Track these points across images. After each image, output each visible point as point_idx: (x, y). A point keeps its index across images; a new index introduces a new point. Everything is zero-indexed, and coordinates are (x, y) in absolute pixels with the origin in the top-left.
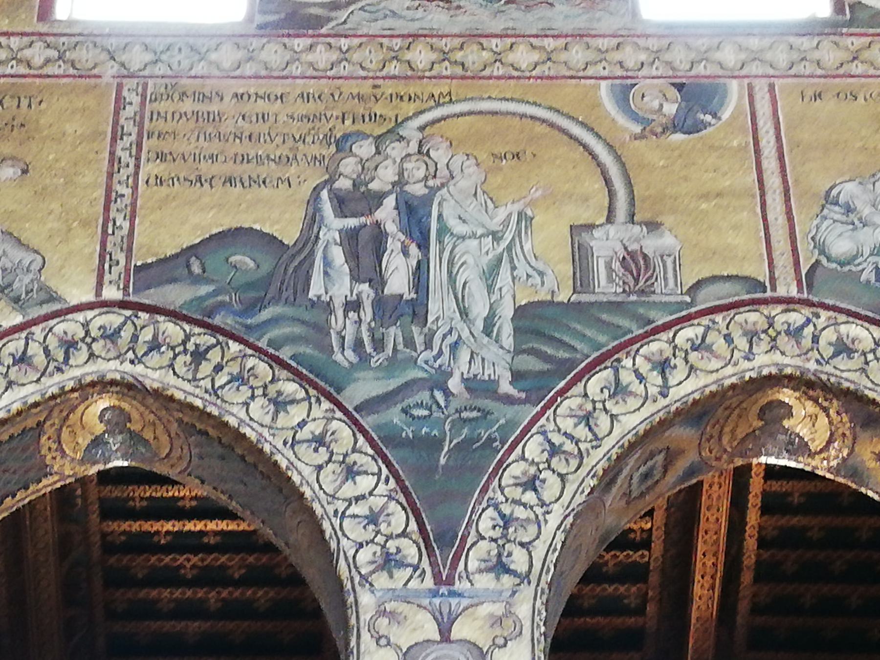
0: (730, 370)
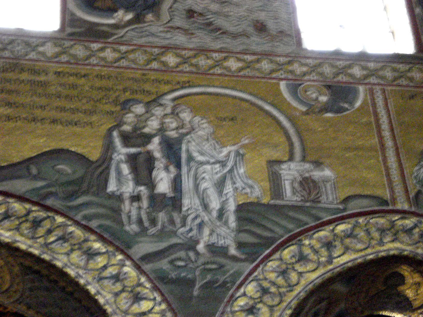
0: (369, 251)
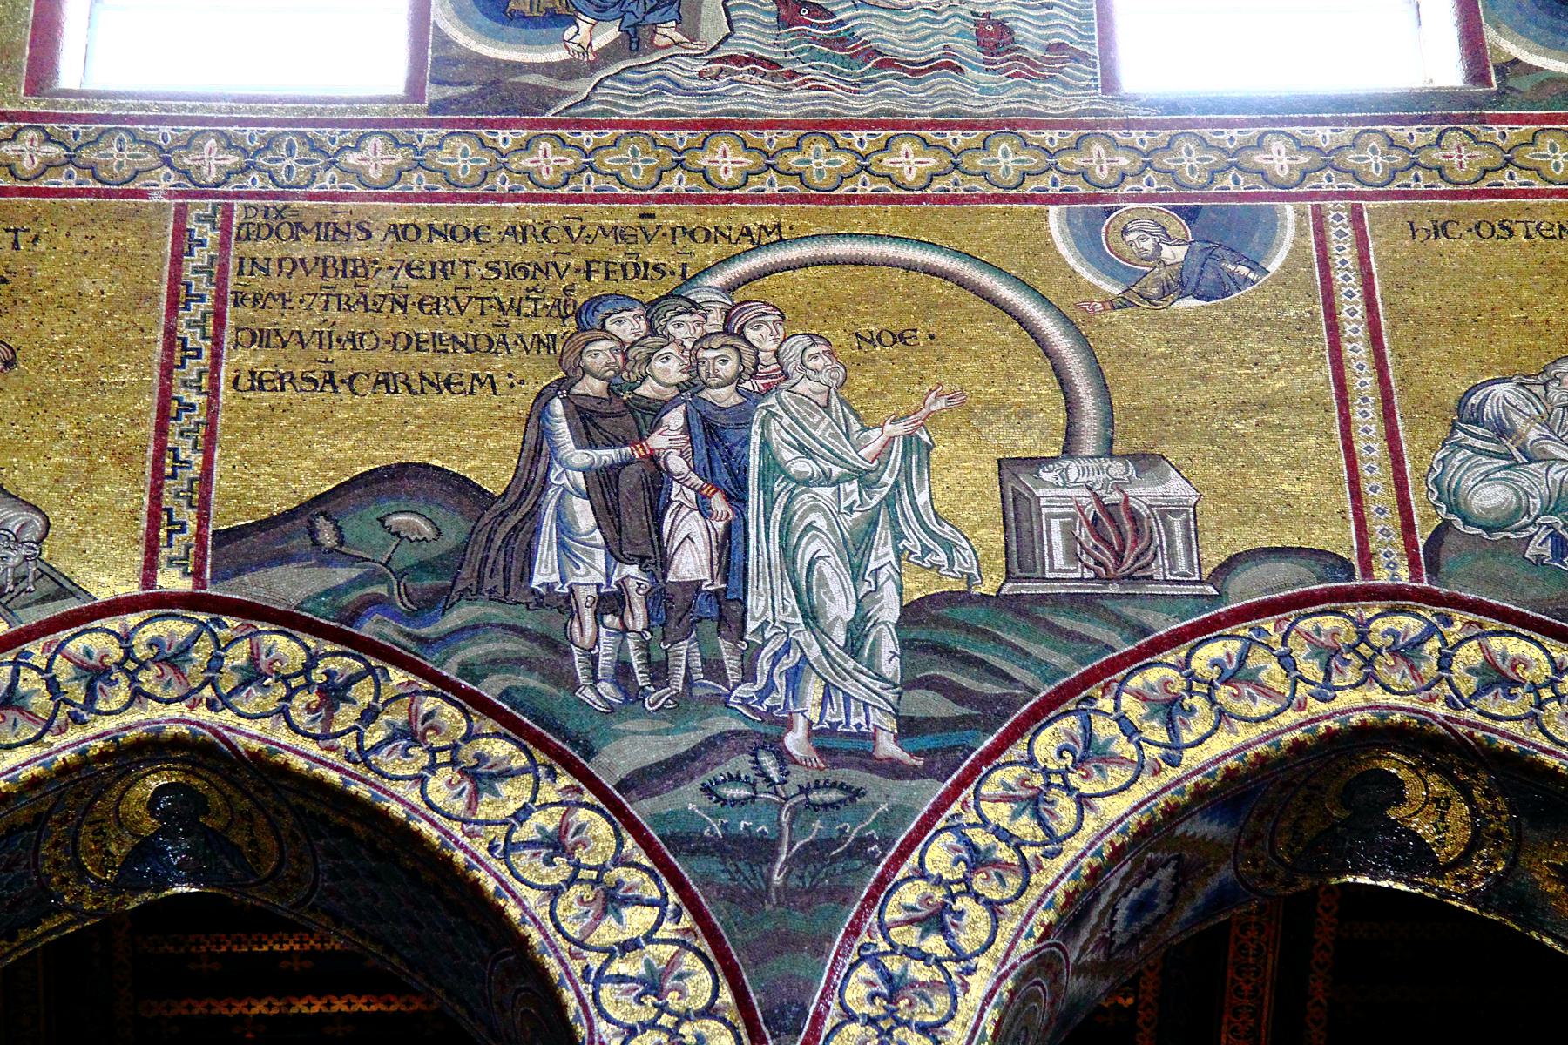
0: (1290, 717)
